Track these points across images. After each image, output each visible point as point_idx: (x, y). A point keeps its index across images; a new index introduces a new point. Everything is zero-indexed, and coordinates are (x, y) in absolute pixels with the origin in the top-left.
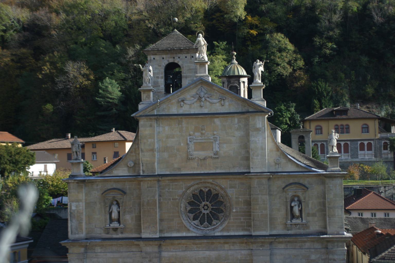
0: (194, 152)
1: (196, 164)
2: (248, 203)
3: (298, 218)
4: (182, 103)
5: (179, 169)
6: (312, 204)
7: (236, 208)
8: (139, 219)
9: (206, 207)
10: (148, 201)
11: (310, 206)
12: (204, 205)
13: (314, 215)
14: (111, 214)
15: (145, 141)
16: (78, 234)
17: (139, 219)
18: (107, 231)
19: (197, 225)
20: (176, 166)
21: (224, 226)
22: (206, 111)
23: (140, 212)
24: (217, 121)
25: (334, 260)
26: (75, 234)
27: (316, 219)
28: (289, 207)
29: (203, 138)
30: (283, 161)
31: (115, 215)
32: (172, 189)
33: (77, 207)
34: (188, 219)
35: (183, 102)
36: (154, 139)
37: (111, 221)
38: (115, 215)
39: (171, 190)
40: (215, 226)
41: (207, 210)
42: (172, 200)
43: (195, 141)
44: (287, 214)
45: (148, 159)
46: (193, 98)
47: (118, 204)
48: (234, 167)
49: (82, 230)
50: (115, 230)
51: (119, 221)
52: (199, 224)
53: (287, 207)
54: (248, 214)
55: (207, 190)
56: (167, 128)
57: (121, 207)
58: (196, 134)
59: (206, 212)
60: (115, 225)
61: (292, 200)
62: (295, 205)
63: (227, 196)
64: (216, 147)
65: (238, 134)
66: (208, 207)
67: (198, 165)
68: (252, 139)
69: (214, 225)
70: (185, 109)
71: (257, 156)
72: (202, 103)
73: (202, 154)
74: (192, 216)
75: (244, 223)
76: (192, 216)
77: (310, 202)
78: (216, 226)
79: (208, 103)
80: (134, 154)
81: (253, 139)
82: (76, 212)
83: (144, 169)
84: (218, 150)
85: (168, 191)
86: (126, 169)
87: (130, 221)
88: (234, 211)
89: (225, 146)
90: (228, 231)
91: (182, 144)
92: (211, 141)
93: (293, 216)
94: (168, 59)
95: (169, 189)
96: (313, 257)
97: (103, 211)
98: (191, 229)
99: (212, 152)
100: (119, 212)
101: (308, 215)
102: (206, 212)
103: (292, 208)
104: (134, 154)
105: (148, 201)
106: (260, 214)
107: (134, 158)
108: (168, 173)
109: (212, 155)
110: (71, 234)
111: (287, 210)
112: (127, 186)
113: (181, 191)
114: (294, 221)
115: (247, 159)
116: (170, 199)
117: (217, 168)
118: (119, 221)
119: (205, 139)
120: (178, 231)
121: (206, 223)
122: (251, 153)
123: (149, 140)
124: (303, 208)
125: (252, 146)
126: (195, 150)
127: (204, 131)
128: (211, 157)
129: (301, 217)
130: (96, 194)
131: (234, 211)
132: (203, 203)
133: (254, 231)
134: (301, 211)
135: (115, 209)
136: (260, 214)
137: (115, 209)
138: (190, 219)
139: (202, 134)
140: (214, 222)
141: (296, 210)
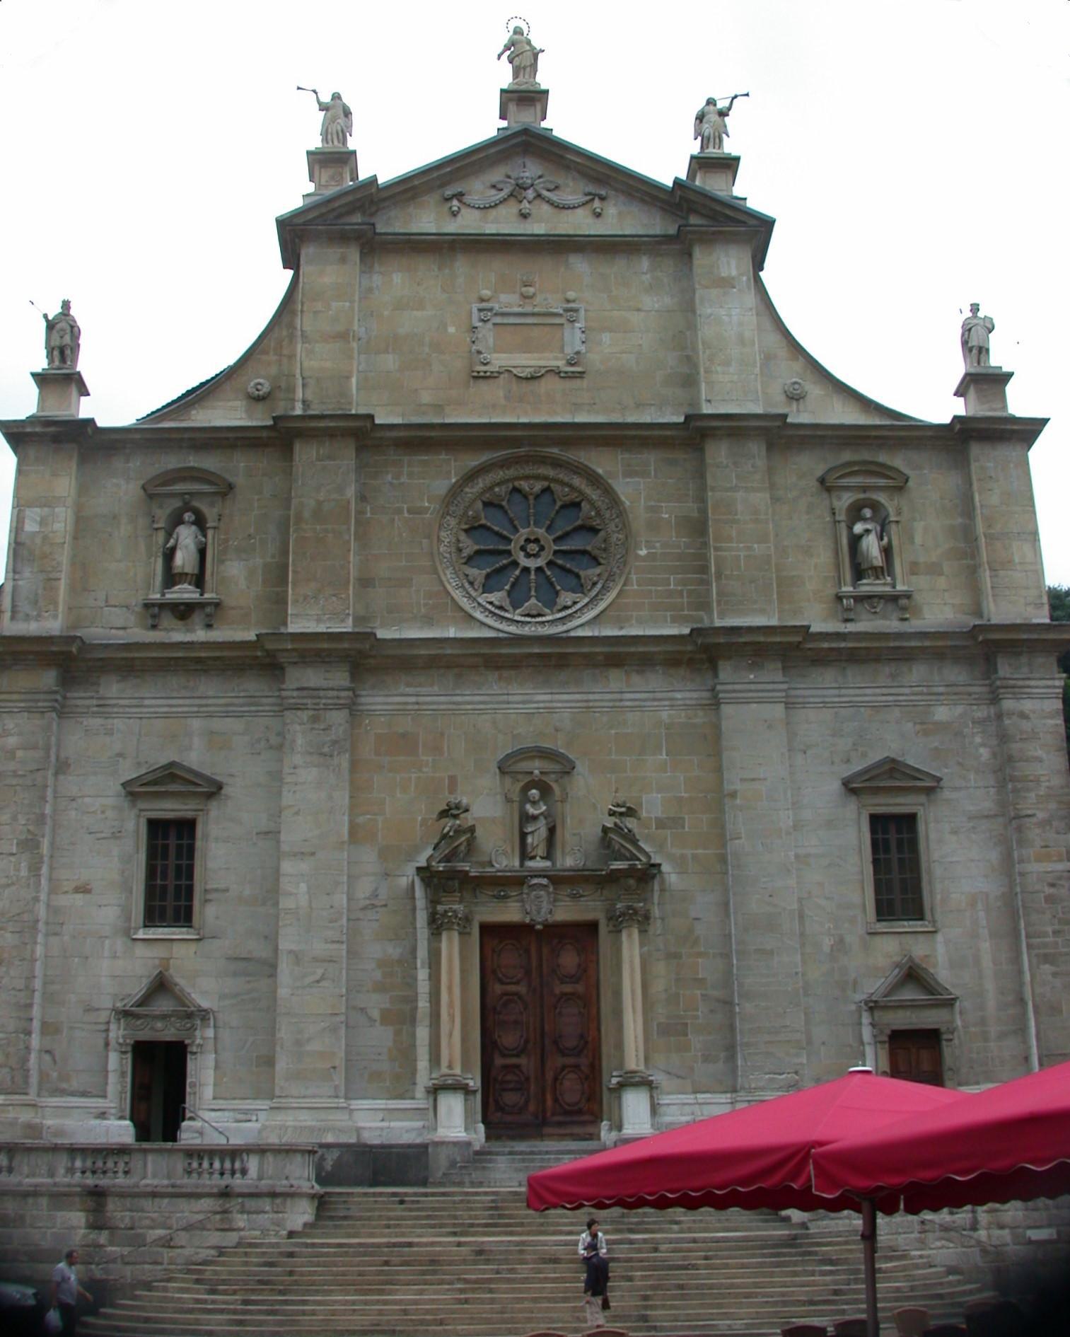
0: (495, 355)
1: (501, 393)
2: (698, 528)
3: (878, 572)
4: (455, 202)
5: (438, 408)
7: (649, 545)
8: (278, 576)
9: (533, 548)
10: (319, 503)
11: (918, 539)
12: (528, 541)
13: (934, 569)
14: (169, 555)
15: (319, 306)
16: (38, 617)
17: (278, 576)
19: (501, 608)
20: (426, 398)
21: (602, 606)
22: (537, 228)
23: (285, 552)
25: (1023, 716)
26: (27, 618)
27: (942, 582)
28: (845, 541)
29: (528, 309)
30: (815, 391)
31: (184, 559)
32: (410, 475)
33: (43, 522)
34: (467, 585)
35: (460, 201)
36: (352, 302)
37: (171, 578)
38: (184, 559)
39: (404, 479)
40: (570, 611)
41: (536, 556)
42: (409, 511)
43: (498, 320)
44: (838, 566)
45: (328, 364)
46: (493, 192)
47: (200, 522)
48: (639, 406)
49: (56, 604)
50: (184, 611)
51: (199, 581)
52: (506, 604)
53: (836, 541)
55: (538, 486)
56: (397, 278)
57: (210, 533)
58: (504, 298)
59: (532, 564)
60: (184, 593)
61: (855, 513)
62: (868, 531)
63: (614, 501)
66: (542, 548)
67: (506, 398)
68: (705, 310)
69: (566, 608)
71: (727, 363)
72: (525, 204)
74: (478, 574)
75: (682, 597)
76: (478, 574)
77: (919, 526)
78: (574, 609)
79: (546, 207)
80: (272, 357)
81: (709, 311)
82: (38, 541)
83: (309, 397)
84: (583, 348)
85: (391, 484)
86: (240, 404)
87: (243, 584)
88: (643, 552)
89: (606, 337)
90: (620, 622)
91: (452, 330)
92: (557, 321)
93: (859, 572)
95: (397, 477)
96: (942, 713)
97: (142, 547)
98: (478, 615)
99: (560, 355)
100: (202, 552)
101: (914, 569)
102: (532, 564)
103: (855, 541)
104: (272, 357)
105: (319, 503)
106: (742, 554)
107: (273, 370)
108: (398, 420)
109: (561, 363)
110: (13, 618)
111: (837, 552)
114: (869, 586)
115: (689, 380)
116: (399, 511)
117: (577, 407)
118: (199, 581)
119: (533, 314)
120: (429, 621)
121: (533, 601)
122: (702, 357)
123: (334, 305)
124: (895, 543)
125: (706, 332)
126: (497, 349)
127: (531, 290)
128: (556, 372)
129: (891, 573)
131: (643, 552)
132: (524, 532)
133: (722, 615)
134: (887, 551)
135: (187, 537)
136: (742, 554)
138: (471, 583)
139: (525, 297)
140: (566, 598)
141: (872, 547)
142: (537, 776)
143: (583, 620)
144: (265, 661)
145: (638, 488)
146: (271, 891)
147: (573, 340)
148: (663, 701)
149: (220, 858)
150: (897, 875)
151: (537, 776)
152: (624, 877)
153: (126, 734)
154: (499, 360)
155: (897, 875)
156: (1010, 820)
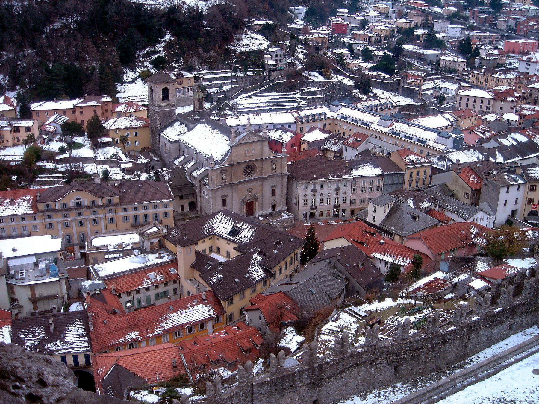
2: (262, 167)
6: (278, 165)
17: (231, 177)
18: (222, 183)
24: (254, 144)
51: (225, 179)
54: (262, 171)
60: (224, 180)
64: (253, 152)
65: (259, 147)
70: (245, 141)
73: (249, 155)
94: (163, 86)
112: (227, 169)
113: (243, 166)
130: (218, 172)
137: (224, 176)
142: (250, 190)
143: (253, 177)
144: (231, 185)
145: (258, 165)
146: (232, 203)
147: (253, 152)
148: (259, 183)
149: (228, 201)
150: (274, 194)
151: (250, 190)
152: (256, 199)
153: (221, 193)
154: (247, 155)
155: (274, 194)
156: (282, 188)
